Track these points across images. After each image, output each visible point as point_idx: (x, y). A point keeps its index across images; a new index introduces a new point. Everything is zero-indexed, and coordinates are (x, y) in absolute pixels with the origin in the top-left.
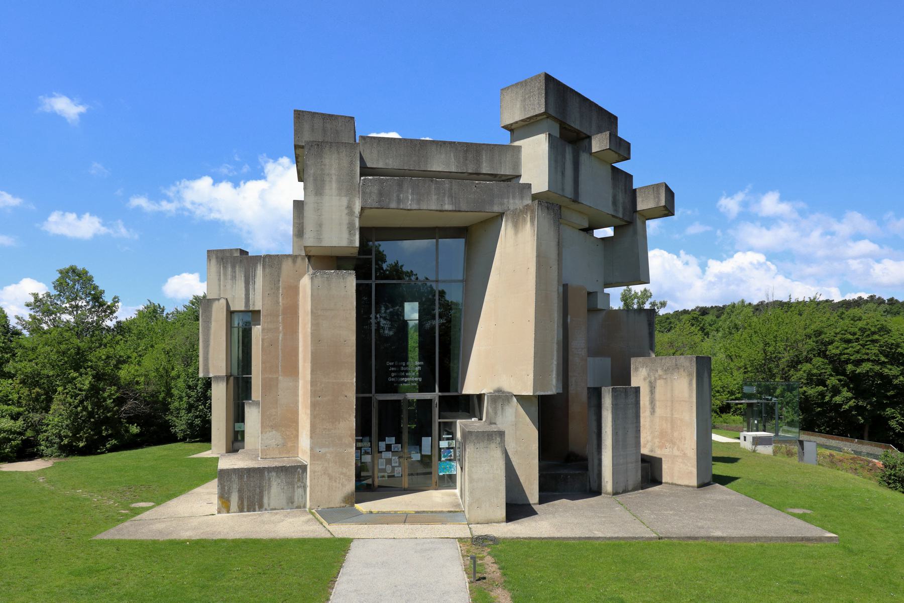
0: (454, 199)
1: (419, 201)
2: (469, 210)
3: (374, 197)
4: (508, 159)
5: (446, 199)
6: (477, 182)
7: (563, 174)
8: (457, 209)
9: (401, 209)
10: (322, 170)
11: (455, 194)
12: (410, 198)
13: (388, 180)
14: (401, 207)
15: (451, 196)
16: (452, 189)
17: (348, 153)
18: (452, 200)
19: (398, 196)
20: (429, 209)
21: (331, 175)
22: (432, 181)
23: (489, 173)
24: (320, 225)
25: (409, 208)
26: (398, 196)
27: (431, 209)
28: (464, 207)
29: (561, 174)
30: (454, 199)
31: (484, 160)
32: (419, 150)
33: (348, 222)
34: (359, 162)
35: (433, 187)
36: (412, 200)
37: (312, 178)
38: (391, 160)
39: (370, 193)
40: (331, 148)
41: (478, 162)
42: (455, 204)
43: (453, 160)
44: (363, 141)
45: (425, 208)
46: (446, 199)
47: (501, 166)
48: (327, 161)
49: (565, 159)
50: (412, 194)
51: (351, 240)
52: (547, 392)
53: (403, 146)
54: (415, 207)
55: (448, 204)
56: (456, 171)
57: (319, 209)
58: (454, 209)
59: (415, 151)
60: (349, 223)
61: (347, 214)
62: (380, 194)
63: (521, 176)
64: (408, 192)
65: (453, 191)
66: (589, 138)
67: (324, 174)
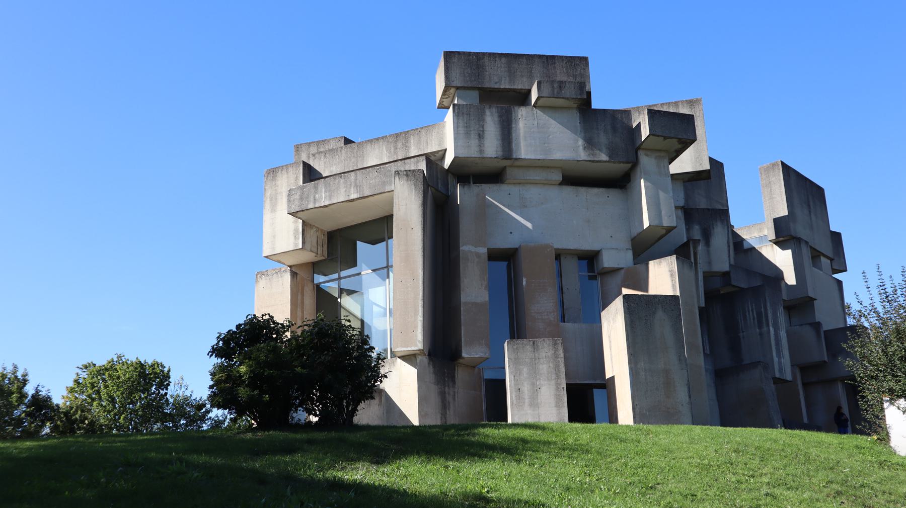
0: (358, 188)
1: (330, 197)
2: (371, 194)
3: (297, 202)
4: (434, 138)
5: (352, 189)
6: (378, 167)
7: (481, 136)
8: (361, 196)
9: (318, 207)
10: (276, 190)
11: (360, 183)
12: (324, 196)
13: (306, 185)
14: (317, 205)
15: (356, 186)
16: (357, 180)
17: (294, 171)
18: (357, 189)
19: (314, 197)
20: (338, 201)
21: (282, 193)
22: (341, 177)
23: (417, 154)
24: (274, 237)
25: (323, 205)
26: (314, 197)
27: (340, 201)
28: (367, 193)
29: (477, 137)
30: (358, 188)
31: (412, 144)
32: (357, 152)
33: (293, 229)
34: (302, 177)
35: (342, 181)
36: (325, 198)
37: (269, 199)
38: (334, 167)
39: (294, 200)
40: (282, 171)
41: (406, 147)
42: (360, 192)
43: (385, 151)
44: (313, 158)
45: (335, 201)
46: (352, 189)
47: (428, 145)
48: (279, 183)
49: (484, 120)
50: (326, 192)
51: (296, 244)
52: (411, 347)
53: (344, 152)
54: (327, 203)
55: (354, 193)
56: (388, 161)
57: (273, 224)
58: (359, 197)
59: (353, 153)
60: (295, 230)
61: (293, 222)
62: (301, 199)
63: (446, 150)
64: (322, 192)
65: (358, 181)
66: (529, 92)
67: (277, 194)
